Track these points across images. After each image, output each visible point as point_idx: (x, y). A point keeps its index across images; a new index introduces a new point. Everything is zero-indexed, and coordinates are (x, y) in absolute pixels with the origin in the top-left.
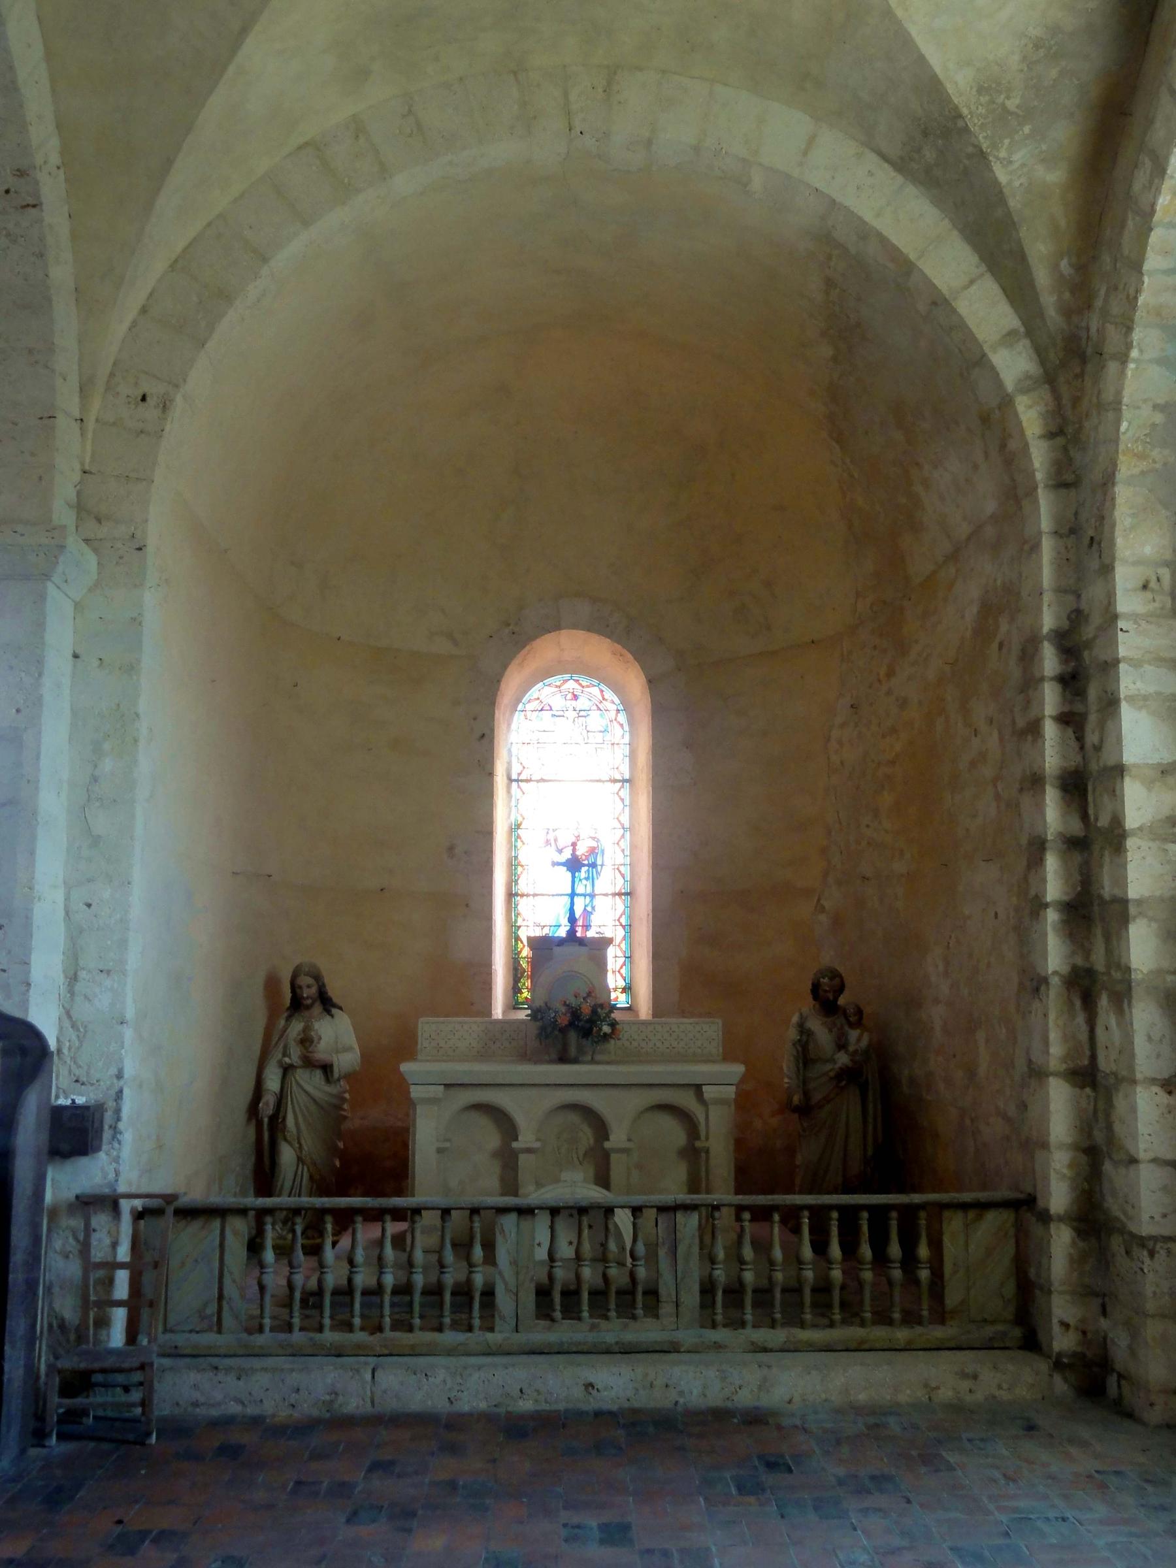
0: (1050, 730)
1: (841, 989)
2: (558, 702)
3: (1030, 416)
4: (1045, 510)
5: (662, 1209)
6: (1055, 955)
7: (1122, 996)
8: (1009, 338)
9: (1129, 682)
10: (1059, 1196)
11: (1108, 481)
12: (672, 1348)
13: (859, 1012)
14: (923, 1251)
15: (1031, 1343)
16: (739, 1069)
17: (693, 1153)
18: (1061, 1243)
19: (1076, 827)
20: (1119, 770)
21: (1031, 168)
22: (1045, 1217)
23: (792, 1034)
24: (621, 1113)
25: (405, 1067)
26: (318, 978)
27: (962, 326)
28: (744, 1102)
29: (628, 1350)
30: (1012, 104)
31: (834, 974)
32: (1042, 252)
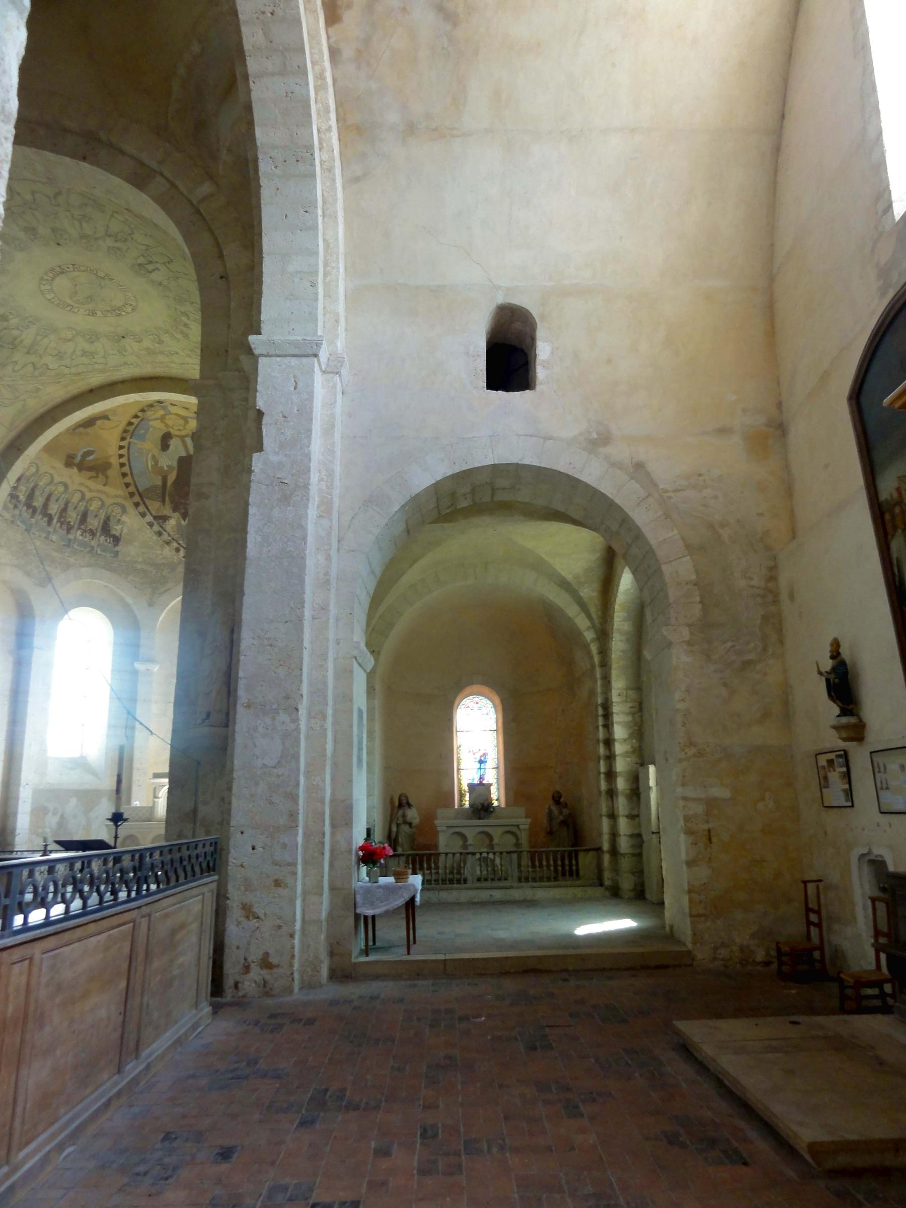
0: (601, 728)
1: (560, 797)
2: (471, 705)
3: (594, 648)
4: (598, 672)
5: (508, 853)
6: (603, 786)
7: (617, 796)
8: (588, 629)
9: (616, 718)
10: (606, 846)
11: (610, 668)
12: (511, 887)
13: (566, 804)
14: (574, 862)
15: (601, 885)
16: (530, 820)
17: (518, 845)
18: (606, 858)
19: (608, 753)
20: (614, 740)
21: (590, 592)
22: (603, 851)
23: (547, 811)
24: (496, 833)
25: (435, 822)
26: (407, 797)
27: (575, 624)
28: (532, 833)
29: (501, 888)
30: (582, 580)
31: (558, 792)
32: (593, 611)
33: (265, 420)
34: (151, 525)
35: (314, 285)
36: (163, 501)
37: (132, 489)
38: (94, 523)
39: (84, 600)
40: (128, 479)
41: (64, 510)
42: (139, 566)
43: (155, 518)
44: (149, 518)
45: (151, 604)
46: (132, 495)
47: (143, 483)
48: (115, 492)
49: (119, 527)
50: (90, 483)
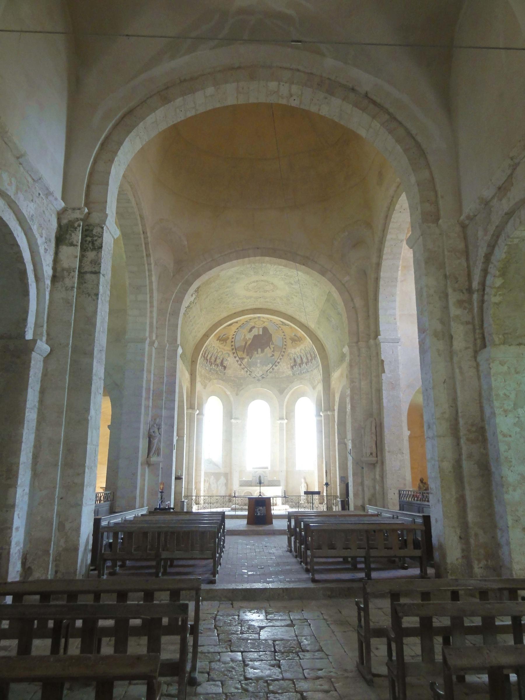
33: (385, 363)
34: (237, 361)
35: (395, 319)
36: (244, 352)
37: (233, 347)
38: (219, 361)
39: (213, 393)
40: (233, 344)
41: (211, 357)
42: (232, 379)
43: (239, 358)
44: (237, 358)
45: (237, 395)
46: (233, 349)
47: (237, 345)
48: (228, 348)
49: (226, 363)
50: (221, 346)
